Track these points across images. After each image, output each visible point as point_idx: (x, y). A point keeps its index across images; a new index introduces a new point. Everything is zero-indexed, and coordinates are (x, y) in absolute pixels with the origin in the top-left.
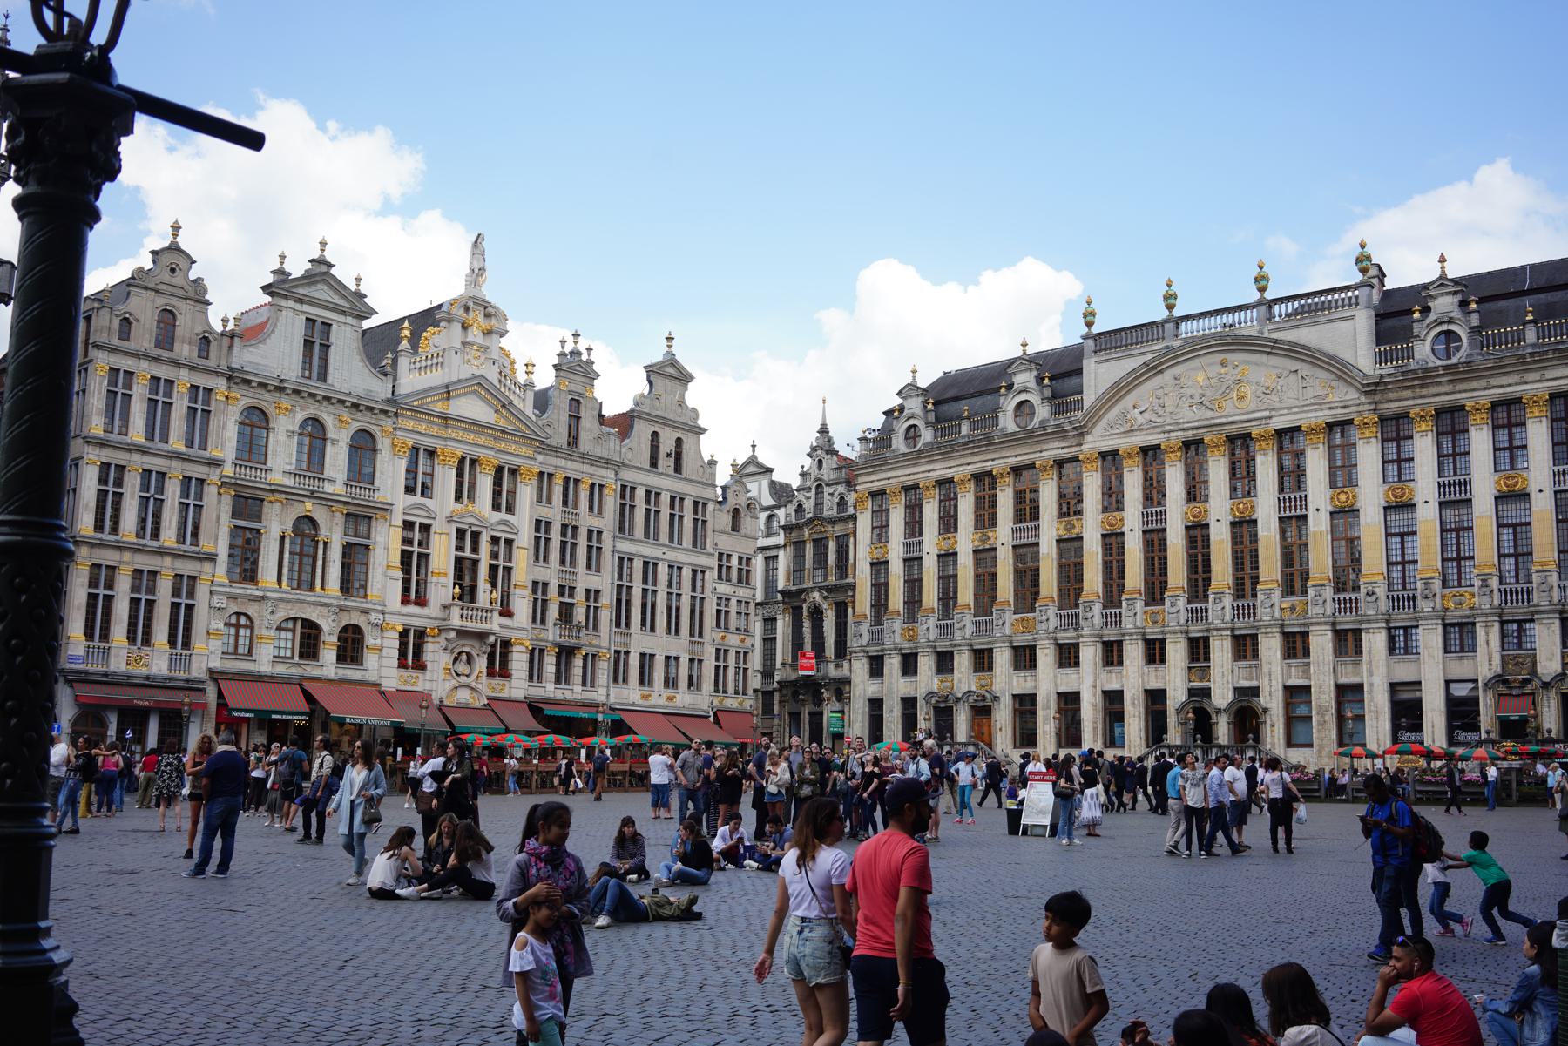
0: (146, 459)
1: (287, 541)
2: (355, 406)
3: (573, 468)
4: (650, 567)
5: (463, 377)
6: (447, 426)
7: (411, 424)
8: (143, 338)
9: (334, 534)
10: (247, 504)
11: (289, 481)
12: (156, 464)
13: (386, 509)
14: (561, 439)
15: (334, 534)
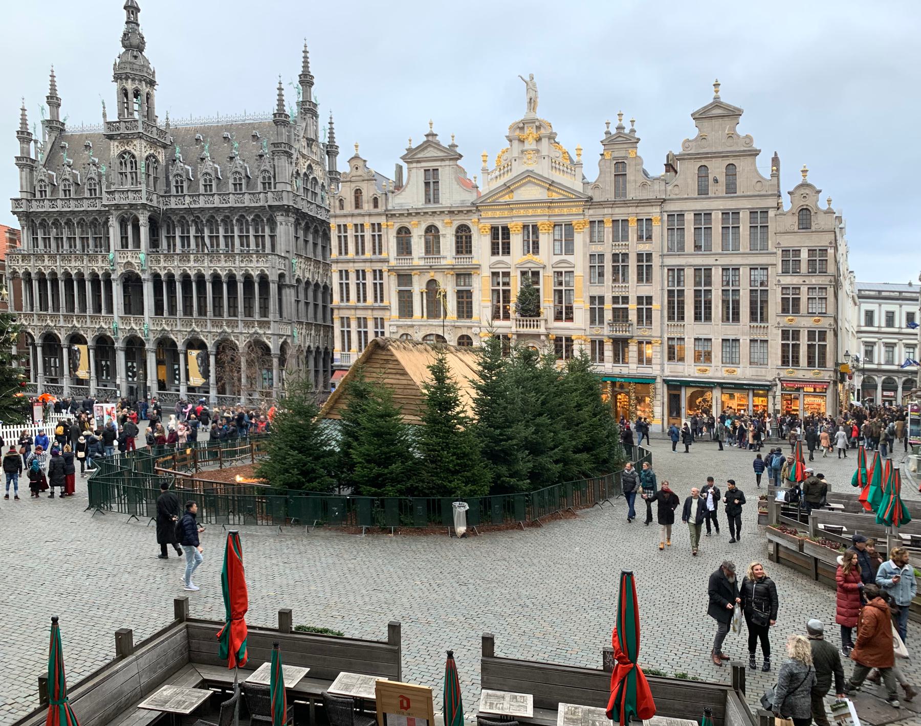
0: (356, 265)
1: (425, 295)
2: (450, 212)
3: (620, 213)
4: (704, 275)
5: (535, 171)
6: (512, 209)
7: (490, 214)
8: (349, 207)
9: (448, 287)
10: (404, 278)
11: (422, 263)
12: (360, 266)
13: (478, 267)
14: (611, 196)
15: (448, 287)
